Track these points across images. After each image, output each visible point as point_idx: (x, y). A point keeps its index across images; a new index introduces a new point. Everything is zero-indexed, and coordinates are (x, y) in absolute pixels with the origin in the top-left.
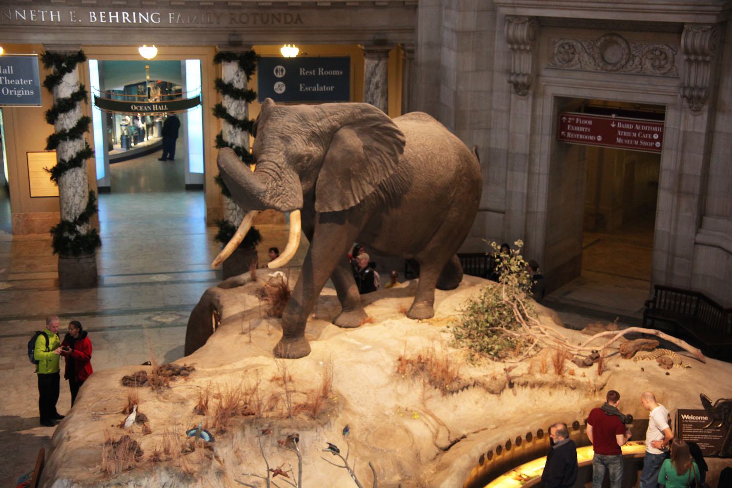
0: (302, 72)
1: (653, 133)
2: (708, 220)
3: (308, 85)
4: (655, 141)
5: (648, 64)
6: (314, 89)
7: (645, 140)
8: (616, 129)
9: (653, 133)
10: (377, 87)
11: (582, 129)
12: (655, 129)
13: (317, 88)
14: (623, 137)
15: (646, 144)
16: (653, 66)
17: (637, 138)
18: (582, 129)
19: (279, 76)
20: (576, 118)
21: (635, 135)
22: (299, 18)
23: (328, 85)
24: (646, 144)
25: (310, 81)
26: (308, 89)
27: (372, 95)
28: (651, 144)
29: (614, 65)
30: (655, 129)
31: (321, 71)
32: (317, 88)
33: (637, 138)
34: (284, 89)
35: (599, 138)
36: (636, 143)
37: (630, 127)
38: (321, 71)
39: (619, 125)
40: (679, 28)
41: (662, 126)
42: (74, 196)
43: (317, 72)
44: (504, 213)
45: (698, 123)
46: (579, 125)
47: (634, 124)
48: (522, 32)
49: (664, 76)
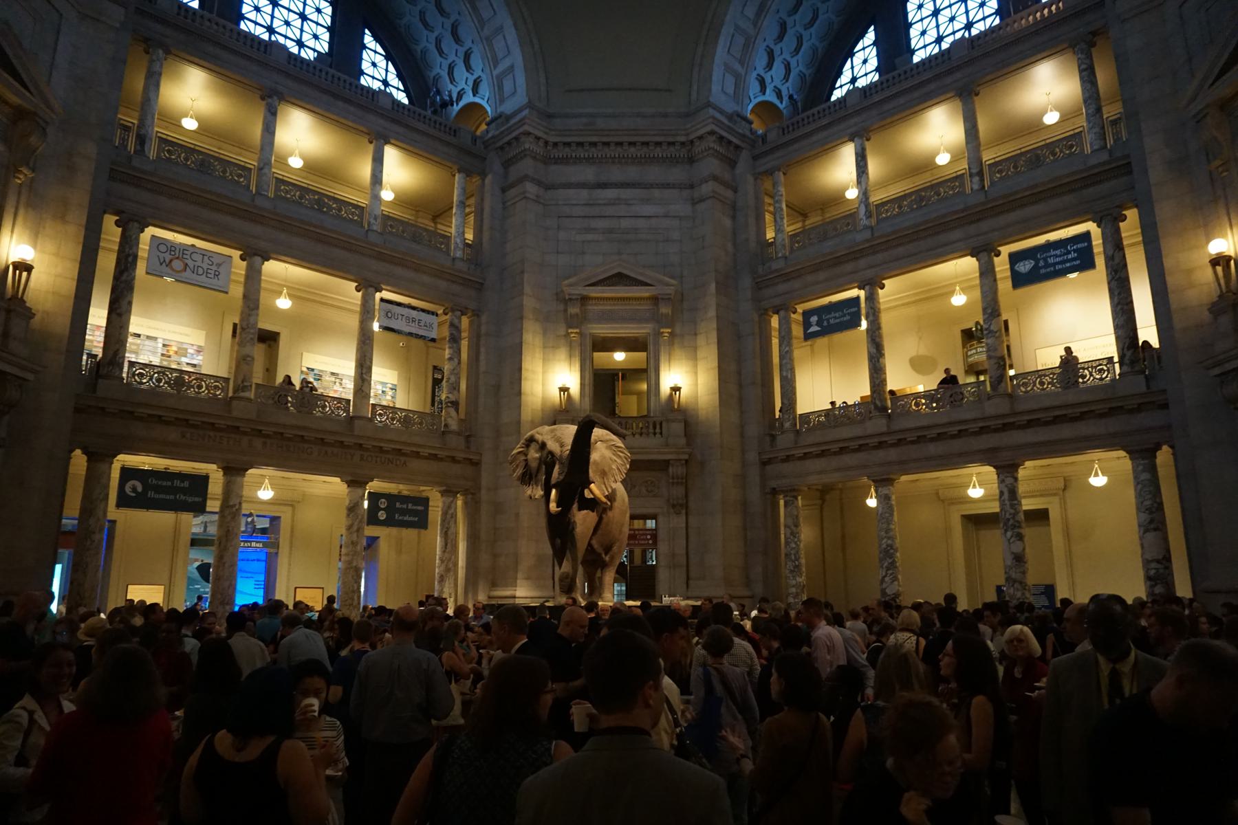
0: (398, 505)
1: (647, 535)
2: (691, 582)
4: (648, 540)
5: (644, 490)
6: (405, 519)
7: (643, 539)
9: (647, 535)
15: (643, 542)
16: (647, 490)
19: (382, 506)
22: (405, 463)
24: (643, 542)
25: (404, 512)
27: (449, 524)
31: (410, 506)
32: (406, 518)
34: (385, 516)
38: (410, 506)
40: (665, 464)
42: (229, 588)
45: (680, 521)
49: (655, 496)
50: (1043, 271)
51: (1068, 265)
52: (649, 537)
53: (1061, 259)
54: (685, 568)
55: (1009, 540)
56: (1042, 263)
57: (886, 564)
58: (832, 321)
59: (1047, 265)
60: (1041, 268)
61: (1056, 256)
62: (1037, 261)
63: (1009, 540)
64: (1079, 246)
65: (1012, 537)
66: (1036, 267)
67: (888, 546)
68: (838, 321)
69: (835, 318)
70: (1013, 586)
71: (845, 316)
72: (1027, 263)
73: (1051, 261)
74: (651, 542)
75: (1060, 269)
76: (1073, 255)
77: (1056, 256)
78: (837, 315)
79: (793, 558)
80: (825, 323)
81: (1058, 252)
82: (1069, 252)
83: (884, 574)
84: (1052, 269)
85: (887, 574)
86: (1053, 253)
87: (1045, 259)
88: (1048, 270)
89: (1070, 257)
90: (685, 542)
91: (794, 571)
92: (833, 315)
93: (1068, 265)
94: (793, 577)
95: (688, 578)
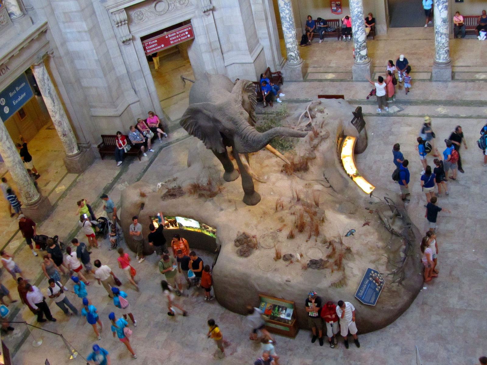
0: (11, 95)
1: (185, 32)
2: (224, 55)
3: (16, 100)
4: (186, 35)
6: (19, 100)
7: (184, 36)
8: (169, 38)
9: (185, 32)
10: (48, 80)
11: (153, 46)
12: (185, 30)
13: (20, 98)
14: (173, 40)
17: (179, 38)
18: (153, 46)
20: (148, 42)
21: (178, 37)
23: (23, 93)
25: (16, 97)
26: (17, 102)
28: (186, 37)
29: (163, 10)
30: (185, 30)
31: (17, 89)
32: (20, 98)
33: (179, 38)
35: (163, 46)
36: (179, 40)
37: (175, 34)
38: (17, 89)
39: (170, 36)
41: (191, 27)
43: (16, 91)
44: (139, 101)
46: (151, 45)
47: (176, 32)
48: (124, 16)
52: (187, 33)
54: (220, 50)
55: (440, 11)
57: (358, 23)
63: (440, 11)
65: (442, 8)
67: (358, 12)
70: (441, 36)
74: (189, 36)
79: (288, 19)
83: (356, 30)
85: (358, 29)
90: (216, 32)
91: (290, 28)
94: (290, 32)
95: (222, 54)
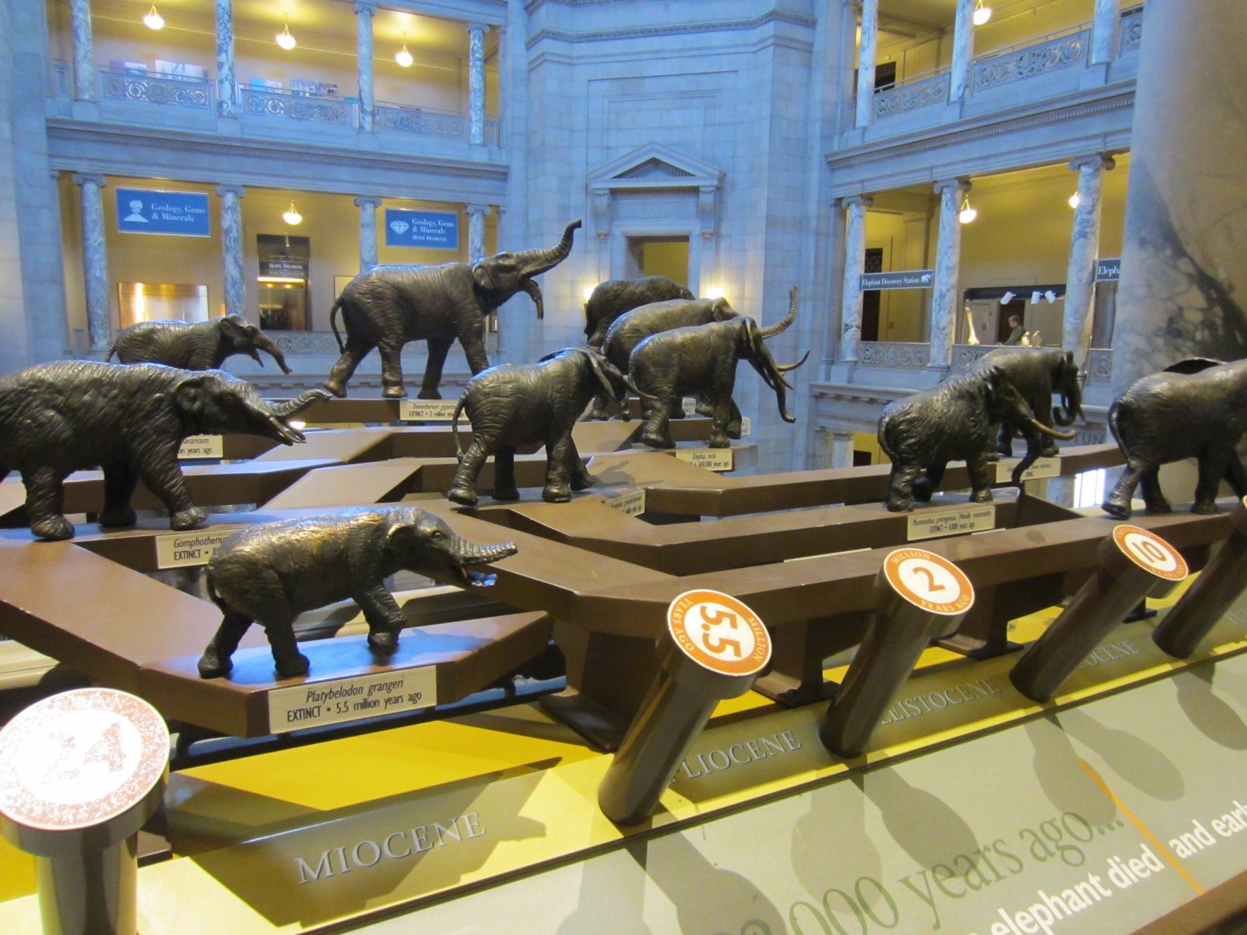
50: (415, 237)
51: (437, 239)
53: (432, 231)
56: (415, 229)
58: (166, 217)
59: (419, 233)
60: (415, 233)
61: (428, 227)
62: (411, 226)
64: (450, 225)
66: (409, 233)
68: (176, 218)
69: (171, 213)
71: (185, 214)
72: (402, 223)
73: (423, 230)
75: (429, 241)
76: (441, 231)
77: (428, 227)
78: (174, 210)
80: (155, 216)
81: (430, 224)
82: (439, 228)
84: (423, 238)
86: (425, 222)
87: (418, 226)
88: (420, 238)
89: (439, 232)
92: (167, 208)
93: (437, 239)
